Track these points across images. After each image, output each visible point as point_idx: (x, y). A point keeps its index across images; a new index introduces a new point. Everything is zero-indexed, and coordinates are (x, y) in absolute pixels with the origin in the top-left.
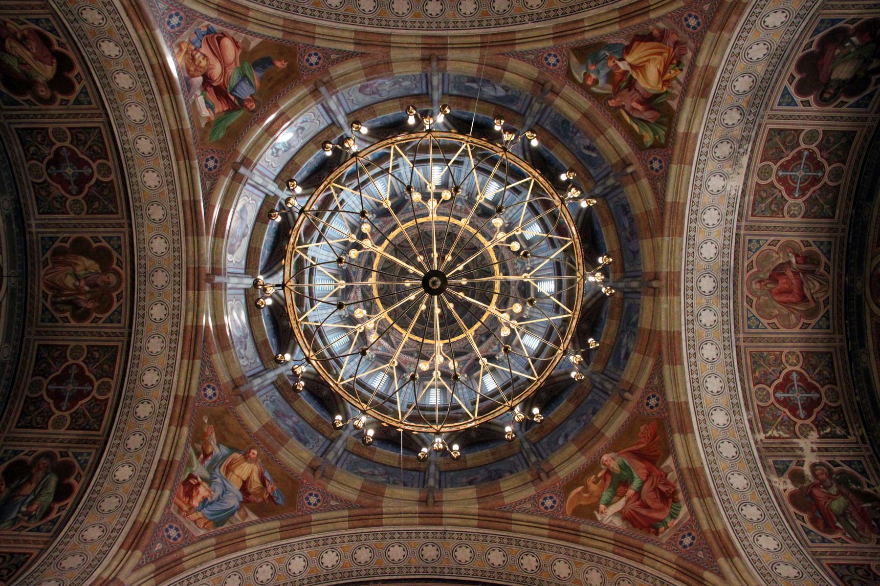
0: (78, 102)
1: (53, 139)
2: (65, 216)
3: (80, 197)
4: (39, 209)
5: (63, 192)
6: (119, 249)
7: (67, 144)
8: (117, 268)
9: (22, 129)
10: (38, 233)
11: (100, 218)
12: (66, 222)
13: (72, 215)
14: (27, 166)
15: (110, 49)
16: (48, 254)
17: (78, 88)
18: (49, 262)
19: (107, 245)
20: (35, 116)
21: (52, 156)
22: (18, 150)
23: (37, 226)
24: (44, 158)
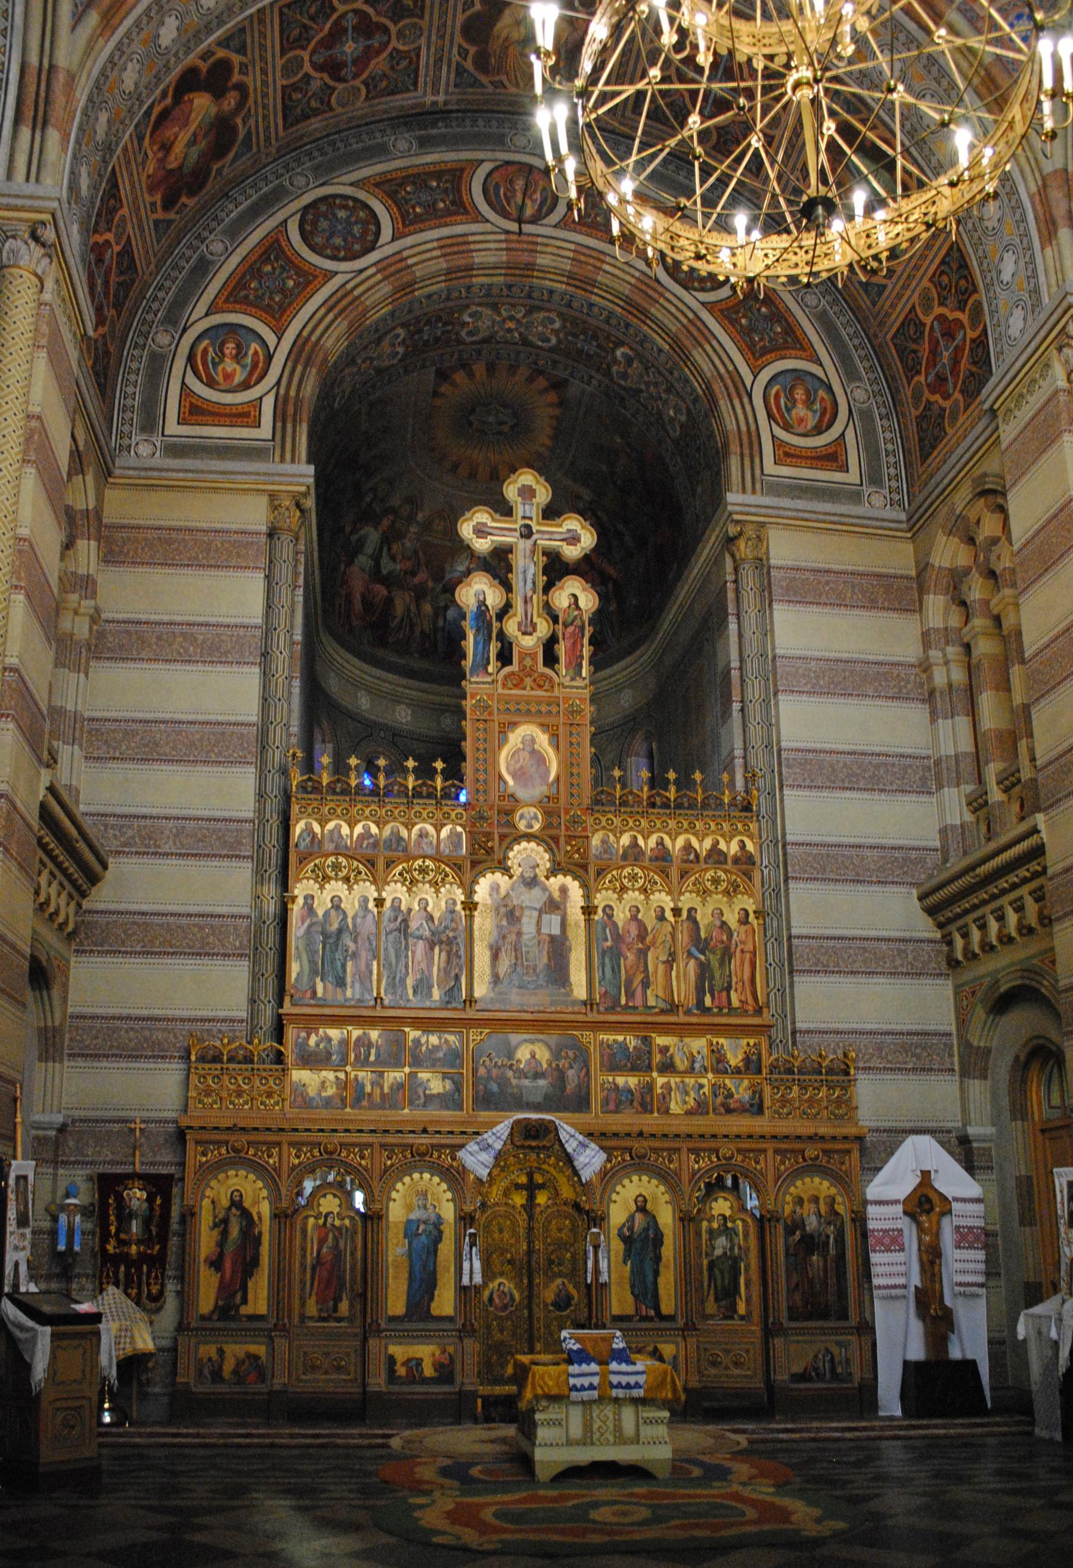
1: (300, 76)
2: (424, 52)
4: (408, 90)
5: (385, 55)
7: (306, 55)
9: (285, 117)
10: (446, 93)
12: (433, 50)
13: (423, 41)
14: (339, 110)
16: (484, 79)
18: (497, 78)
20: (265, 107)
21: (325, 76)
22: (315, 124)
23: (436, 91)
24: (329, 87)
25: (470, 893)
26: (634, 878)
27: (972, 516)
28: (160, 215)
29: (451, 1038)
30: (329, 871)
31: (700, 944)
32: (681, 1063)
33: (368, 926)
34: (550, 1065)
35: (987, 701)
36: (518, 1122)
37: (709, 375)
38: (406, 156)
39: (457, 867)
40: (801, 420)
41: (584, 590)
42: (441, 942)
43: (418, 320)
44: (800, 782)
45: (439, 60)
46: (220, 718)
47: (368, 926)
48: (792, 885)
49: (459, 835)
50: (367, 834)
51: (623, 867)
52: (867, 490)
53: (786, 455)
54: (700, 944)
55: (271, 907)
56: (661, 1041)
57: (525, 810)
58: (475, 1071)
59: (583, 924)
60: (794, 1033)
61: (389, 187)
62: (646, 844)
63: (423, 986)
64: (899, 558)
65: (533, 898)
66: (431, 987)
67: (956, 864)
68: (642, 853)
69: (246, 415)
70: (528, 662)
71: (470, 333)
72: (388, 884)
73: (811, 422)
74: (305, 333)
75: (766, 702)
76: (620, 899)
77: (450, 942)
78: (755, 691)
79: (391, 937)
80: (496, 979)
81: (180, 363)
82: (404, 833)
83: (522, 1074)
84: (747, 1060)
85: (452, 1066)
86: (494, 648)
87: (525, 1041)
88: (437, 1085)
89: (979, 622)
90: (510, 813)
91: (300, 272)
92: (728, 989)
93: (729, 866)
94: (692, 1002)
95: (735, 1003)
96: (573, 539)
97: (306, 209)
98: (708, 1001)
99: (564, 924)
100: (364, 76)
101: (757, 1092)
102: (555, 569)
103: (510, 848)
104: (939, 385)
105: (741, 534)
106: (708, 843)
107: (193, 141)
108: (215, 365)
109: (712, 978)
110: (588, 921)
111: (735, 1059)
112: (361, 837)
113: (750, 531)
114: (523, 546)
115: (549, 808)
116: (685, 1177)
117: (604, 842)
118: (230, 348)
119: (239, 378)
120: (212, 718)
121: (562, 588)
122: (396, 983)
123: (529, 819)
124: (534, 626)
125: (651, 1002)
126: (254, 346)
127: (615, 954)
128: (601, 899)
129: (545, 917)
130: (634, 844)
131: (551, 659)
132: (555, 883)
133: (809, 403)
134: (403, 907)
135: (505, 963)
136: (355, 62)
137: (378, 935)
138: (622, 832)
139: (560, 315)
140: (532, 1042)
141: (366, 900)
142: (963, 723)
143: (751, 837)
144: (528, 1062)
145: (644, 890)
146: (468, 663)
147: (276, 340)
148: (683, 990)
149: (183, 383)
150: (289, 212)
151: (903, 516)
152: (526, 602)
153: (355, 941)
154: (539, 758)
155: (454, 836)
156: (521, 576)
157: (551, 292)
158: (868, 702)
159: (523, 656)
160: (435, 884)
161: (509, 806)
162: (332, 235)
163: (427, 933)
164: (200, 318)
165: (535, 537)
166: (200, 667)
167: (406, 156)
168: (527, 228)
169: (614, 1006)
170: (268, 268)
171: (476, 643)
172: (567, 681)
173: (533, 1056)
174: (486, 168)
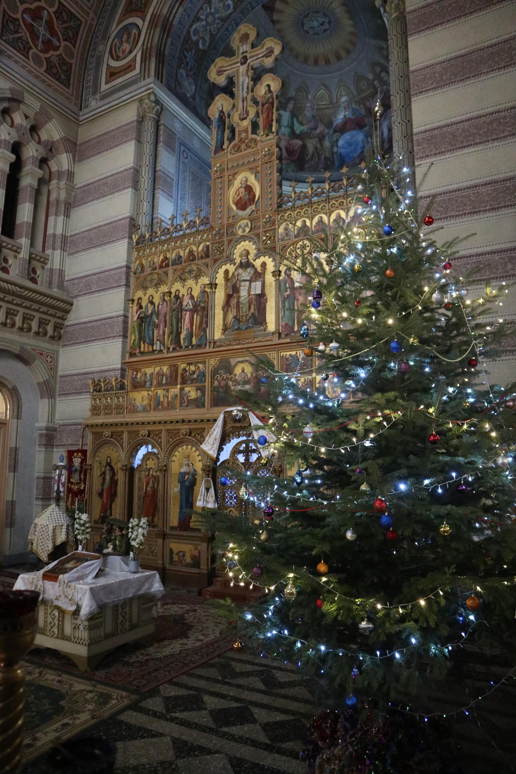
29: (201, 366)
33: (164, 309)
34: (252, 375)
41: (273, 79)
44: (428, 153)
46: (115, 219)
49: (208, 247)
50: (166, 258)
51: (297, 242)
57: (242, 222)
58: (212, 383)
59: (274, 284)
62: (311, 223)
65: (246, 274)
70: (243, 135)
72: (173, 284)
74: (155, 12)
75: (407, 107)
77: (203, 308)
79: (174, 312)
80: (225, 329)
82: (182, 254)
85: (201, 381)
87: (239, 362)
90: (232, 226)
96: (271, 52)
110: (278, 281)
112: (163, 261)
114: (243, 69)
117: (286, 229)
119: (127, 51)
120: (112, 220)
121: (261, 84)
123: (243, 226)
124: (247, 113)
129: (253, 284)
134: (181, 296)
135: (230, 317)
138: (296, 221)
144: (240, 375)
147: (141, 22)
149: (108, 64)
152: (243, 101)
153: (158, 319)
154: (249, 189)
156: (241, 88)
158: (483, 77)
163: (191, 307)
164: (114, 30)
165: (249, 61)
166: (109, 197)
171: (218, 135)
173: (243, 371)
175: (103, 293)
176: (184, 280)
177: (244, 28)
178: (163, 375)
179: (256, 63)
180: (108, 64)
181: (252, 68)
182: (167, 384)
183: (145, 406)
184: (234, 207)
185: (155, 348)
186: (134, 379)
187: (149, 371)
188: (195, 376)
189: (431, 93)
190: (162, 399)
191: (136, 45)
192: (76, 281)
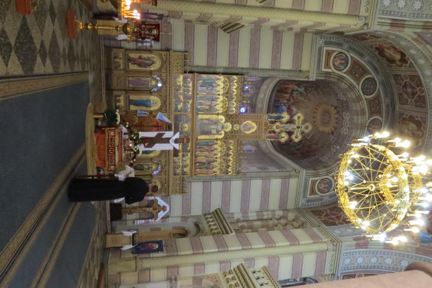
0: (409, 66)
2: (408, 106)
3: (413, 100)
5: (407, 98)
6: (425, 122)
7: (408, 80)
8: (423, 130)
11: (418, 109)
13: (410, 106)
15: (413, 52)
17: (409, 62)
19: (421, 120)
21: (404, 84)
25: (221, 114)
26: (224, 149)
27: (299, 221)
28: (374, 46)
29: (190, 110)
30: (226, 84)
31: (209, 163)
32: (184, 159)
35: (259, 223)
36: (172, 124)
37: (332, 166)
38: (384, 101)
39: (226, 112)
40: (321, 186)
42: (210, 108)
43: (348, 103)
45: (405, 109)
47: (214, 92)
48: (222, 182)
50: (233, 92)
52: (305, 199)
53: (314, 182)
54: (209, 163)
55: (218, 70)
56: (189, 154)
60: (191, 182)
61: (378, 97)
63: (201, 104)
64: (291, 205)
65: (219, 128)
66: (201, 105)
67: (226, 216)
68: (229, 151)
69: (327, 65)
70: (270, 127)
71: (344, 114)
73: (321, 188)
75: (261, 177)
76: (219, 146)
77: (210, 110)
78: (263, 174)
80: (202, 119)
81: (340, 50)
82: (234, 100)
83: (182, 125)
84: (185, 172)
86: (273, 120)
88: (180, 107)
89: (276, 222)
90: (238, 123)
91: (359, 78)
92: (200, 168)
93: (226, 169)
94: (197, 161)
95: (197, 170)
97: (374, 79)
98: (197, 164)
99: (214, 134)
100: (403, 93)
101: (178, 174)
102: (290, 133)
103: (230, 123)
104: (327, 215)
105: (297, 173)
106: (231, 165)
107: (390, 54)
108: (339, 58)
109: (202, 165)
110: (214, 139)
111: (185, 170)
112: (233, 91)
113: (297, 174)
114: (295, 127)
115: (239, 131)
116: (161, 159)
117: (231, 143)
118: (343, 62)
122: (201, 98)
123: (237, 127)
124: (278, 129)
125: (197, 152)
126: (343, 67)
127: (208, 145)
128: (219, 142)
130: (231, 149)
131: (270, 132)
132: (223, 132)
133: (325, 187)
136: (406, 91)
137: (212, 94)
139: (347, 135)
140: (189, 127)
141: (219, 92)
142: (255, 218)
143: (232, 174)
145: (221, 151)
146: (270, 115)
148: (200, 159)
149: (335, 51)
150: (373, 75)
151: (300, 207)
154: (249, 129)
155: (233, 111)
157: (352, 133)
159: (271, 126)
160: (223, 107)
161: (239, 123)
162: (367, 85)
164: (350, 55)
166: (271, 55)
167: (384, 101)
168: (366, 128)
169: (196, 144)
170: (361, 70)
172: (266, 135)
173: (186, 127)
174: (381, 119)
175: (228, 53)
176: (223, 102)
177: (310, 128)
178: (188, 92)
179: (295, 132)
180: (335, 51)
181: (293, 131)
182: (184, 93)
183: (176, 83)
184: (244, 123)
185: (199, 88)
186: (188, 77)
187: (191, 85)
188: (186, 107)
189: (261, 185)
190: (179, 92)
191: (335, 68)
192: (238, 35)
